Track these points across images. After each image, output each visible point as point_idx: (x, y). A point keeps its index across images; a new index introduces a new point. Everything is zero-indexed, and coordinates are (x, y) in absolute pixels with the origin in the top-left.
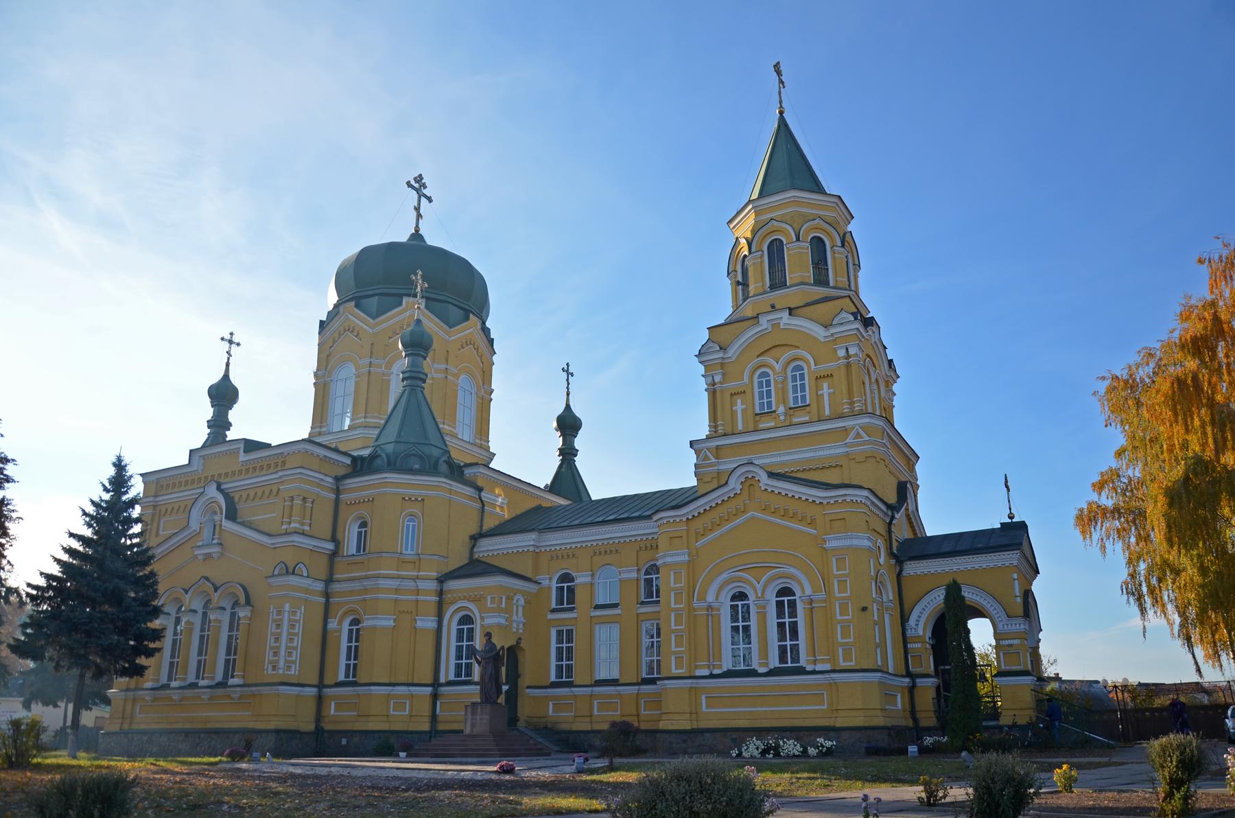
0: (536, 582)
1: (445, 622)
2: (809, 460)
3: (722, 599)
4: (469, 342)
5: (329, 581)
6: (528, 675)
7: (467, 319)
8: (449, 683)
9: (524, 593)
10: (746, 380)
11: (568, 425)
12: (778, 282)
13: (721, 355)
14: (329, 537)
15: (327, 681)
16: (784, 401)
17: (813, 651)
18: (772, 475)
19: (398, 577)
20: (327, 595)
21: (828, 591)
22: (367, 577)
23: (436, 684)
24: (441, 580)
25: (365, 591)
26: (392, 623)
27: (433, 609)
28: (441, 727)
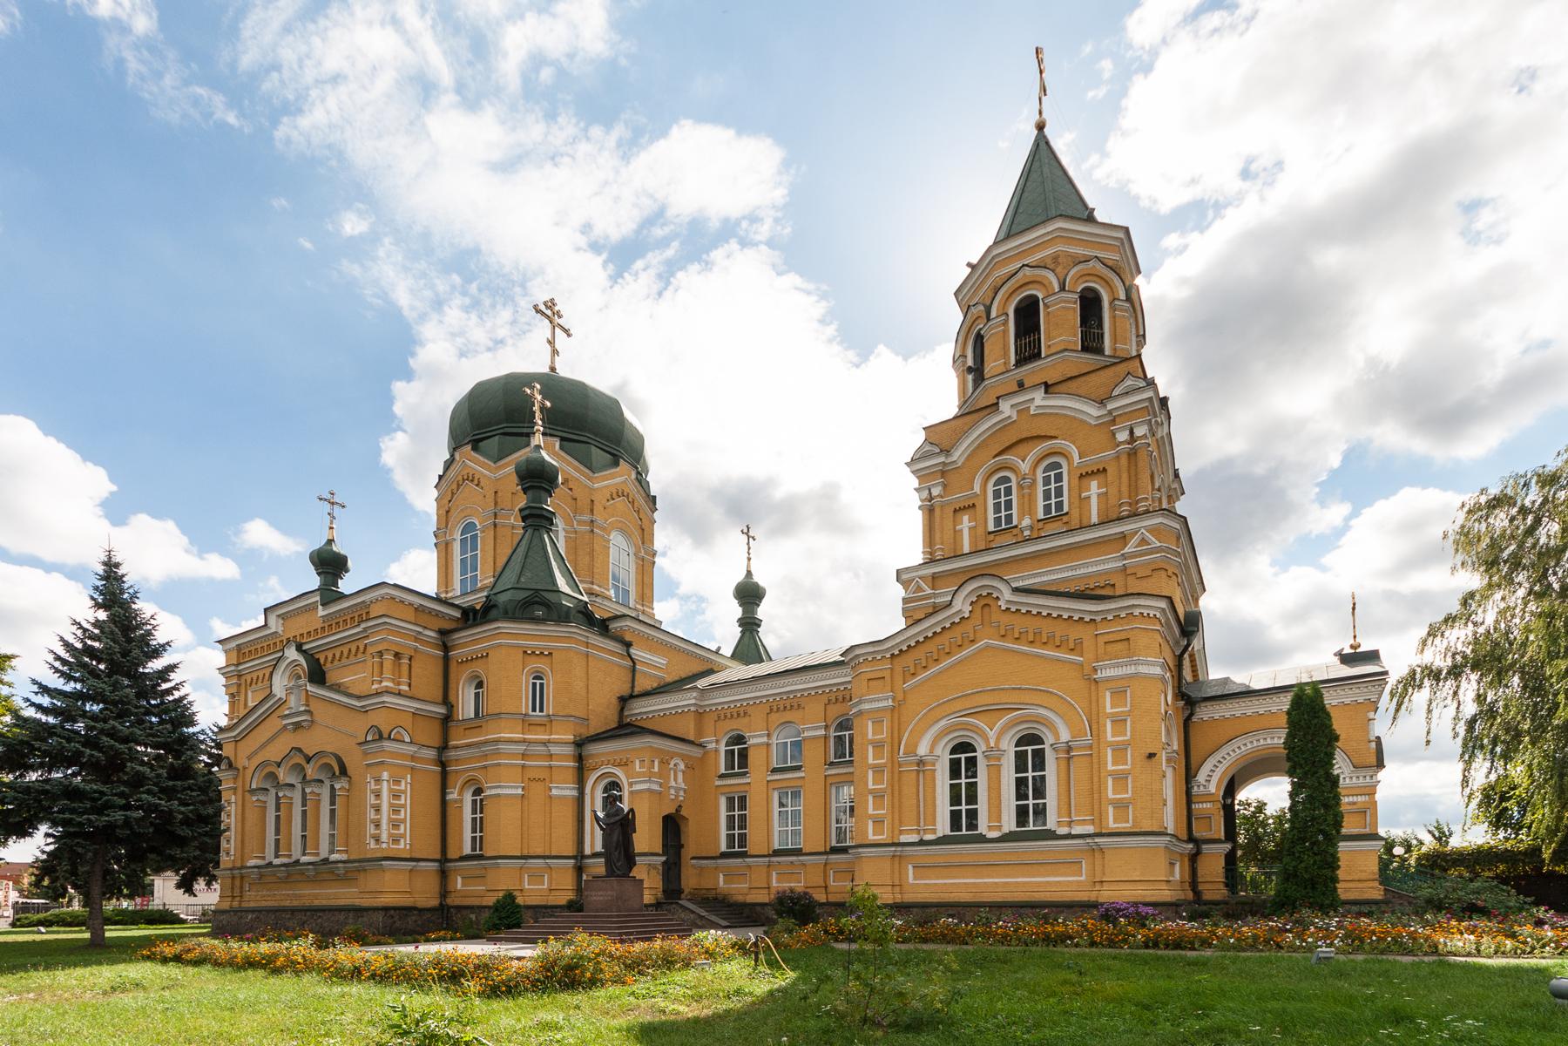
5: (444, 747)
13: (942, 459)
14: (440, 699)
20: (443, 765)
24: (580, 744)
26: (520, 791)
27: (571, 775)
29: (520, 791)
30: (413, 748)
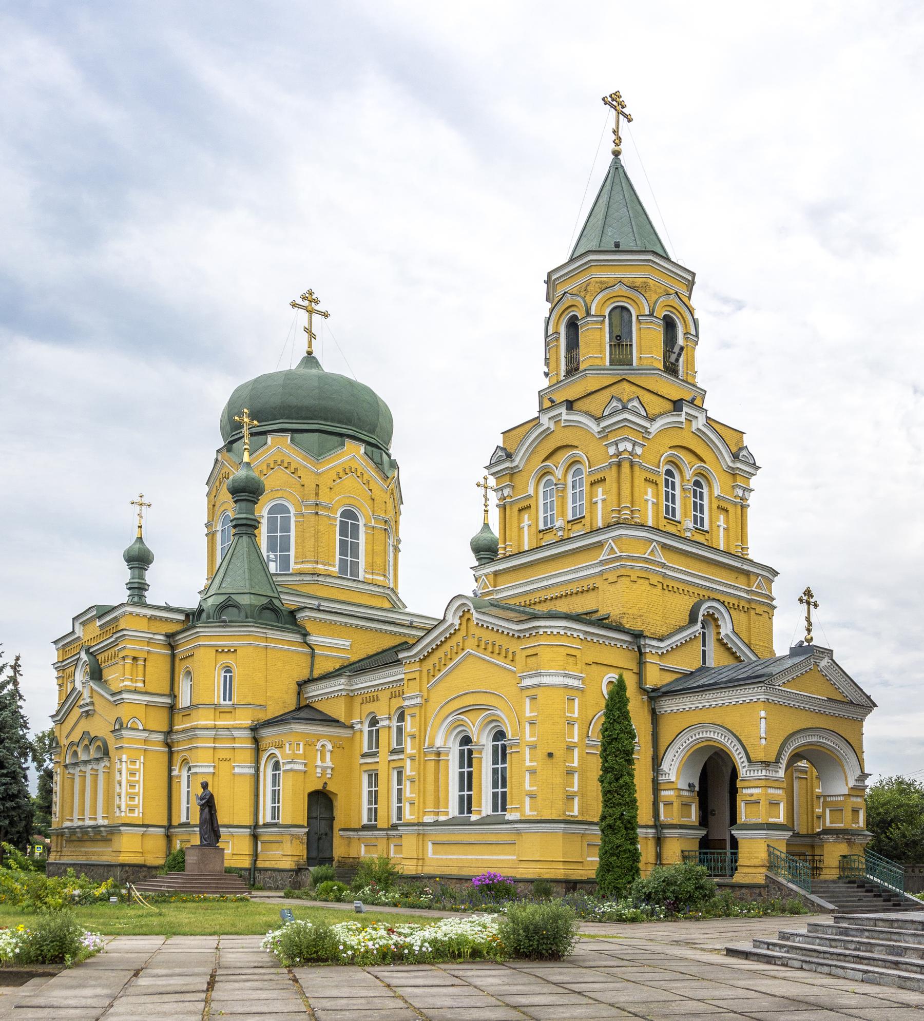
1: (262, 769)
3: (450, 744)
6: (341, 817)
8: (266, 825)
10: (531, 491)
15: (175, 823)
16: (563, 513)
19: (215, 728)
27: (248, 755)
28: (260, 864)
29: (211, 770)
30: (146, 734)
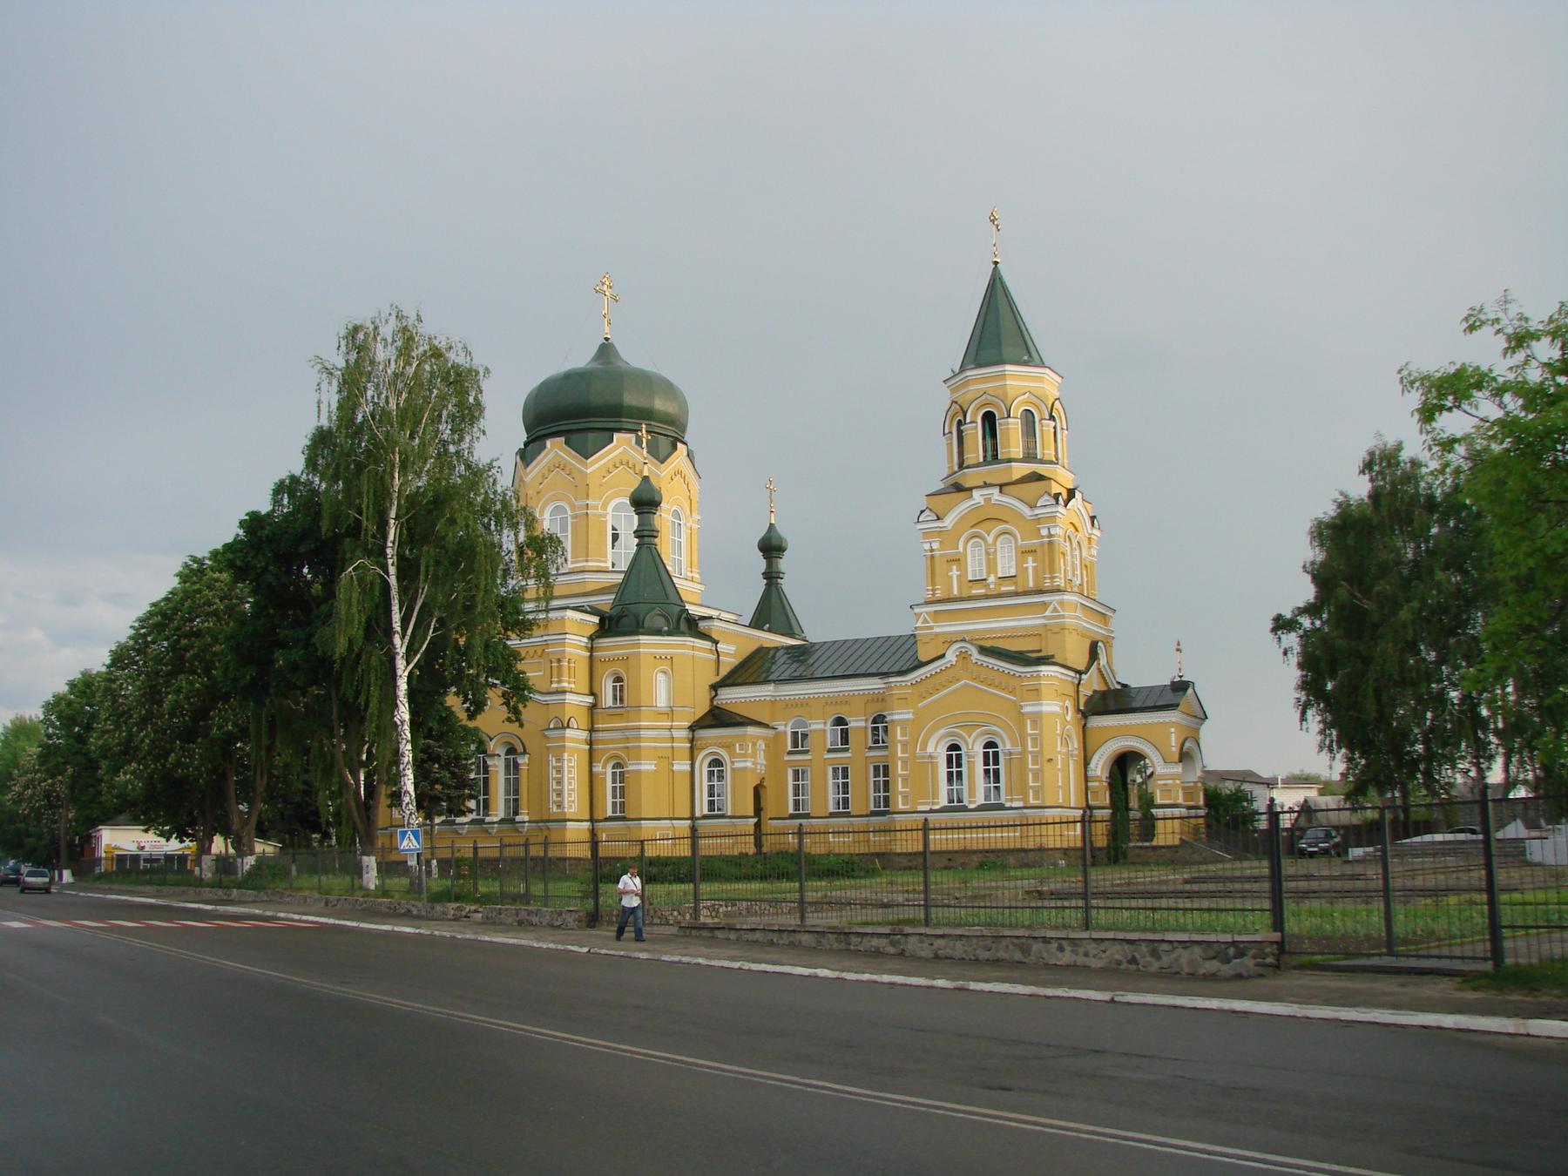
0: (766, 726)
2: (1013, 628)
4: (678, 473)
7: (675, 448)
8: (705, 817)
9: (764, 738)
11: (771, 548)
12: (992, 456)
17: (1010, 791)
18: (984, 650)
20: (591, 743)
21: (1024, 745)
22: (627, 728)
23: (692, 818)
24: (692, 728)
25: (627, 739)
27: (687, 754)
